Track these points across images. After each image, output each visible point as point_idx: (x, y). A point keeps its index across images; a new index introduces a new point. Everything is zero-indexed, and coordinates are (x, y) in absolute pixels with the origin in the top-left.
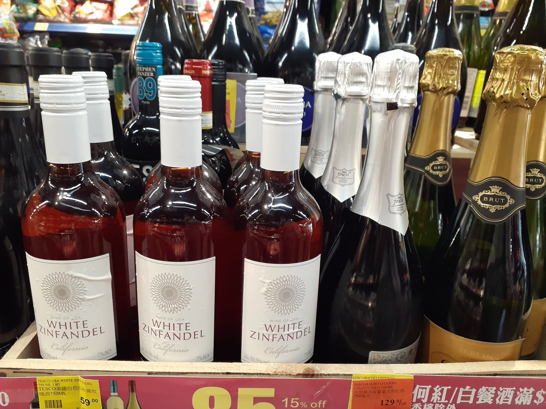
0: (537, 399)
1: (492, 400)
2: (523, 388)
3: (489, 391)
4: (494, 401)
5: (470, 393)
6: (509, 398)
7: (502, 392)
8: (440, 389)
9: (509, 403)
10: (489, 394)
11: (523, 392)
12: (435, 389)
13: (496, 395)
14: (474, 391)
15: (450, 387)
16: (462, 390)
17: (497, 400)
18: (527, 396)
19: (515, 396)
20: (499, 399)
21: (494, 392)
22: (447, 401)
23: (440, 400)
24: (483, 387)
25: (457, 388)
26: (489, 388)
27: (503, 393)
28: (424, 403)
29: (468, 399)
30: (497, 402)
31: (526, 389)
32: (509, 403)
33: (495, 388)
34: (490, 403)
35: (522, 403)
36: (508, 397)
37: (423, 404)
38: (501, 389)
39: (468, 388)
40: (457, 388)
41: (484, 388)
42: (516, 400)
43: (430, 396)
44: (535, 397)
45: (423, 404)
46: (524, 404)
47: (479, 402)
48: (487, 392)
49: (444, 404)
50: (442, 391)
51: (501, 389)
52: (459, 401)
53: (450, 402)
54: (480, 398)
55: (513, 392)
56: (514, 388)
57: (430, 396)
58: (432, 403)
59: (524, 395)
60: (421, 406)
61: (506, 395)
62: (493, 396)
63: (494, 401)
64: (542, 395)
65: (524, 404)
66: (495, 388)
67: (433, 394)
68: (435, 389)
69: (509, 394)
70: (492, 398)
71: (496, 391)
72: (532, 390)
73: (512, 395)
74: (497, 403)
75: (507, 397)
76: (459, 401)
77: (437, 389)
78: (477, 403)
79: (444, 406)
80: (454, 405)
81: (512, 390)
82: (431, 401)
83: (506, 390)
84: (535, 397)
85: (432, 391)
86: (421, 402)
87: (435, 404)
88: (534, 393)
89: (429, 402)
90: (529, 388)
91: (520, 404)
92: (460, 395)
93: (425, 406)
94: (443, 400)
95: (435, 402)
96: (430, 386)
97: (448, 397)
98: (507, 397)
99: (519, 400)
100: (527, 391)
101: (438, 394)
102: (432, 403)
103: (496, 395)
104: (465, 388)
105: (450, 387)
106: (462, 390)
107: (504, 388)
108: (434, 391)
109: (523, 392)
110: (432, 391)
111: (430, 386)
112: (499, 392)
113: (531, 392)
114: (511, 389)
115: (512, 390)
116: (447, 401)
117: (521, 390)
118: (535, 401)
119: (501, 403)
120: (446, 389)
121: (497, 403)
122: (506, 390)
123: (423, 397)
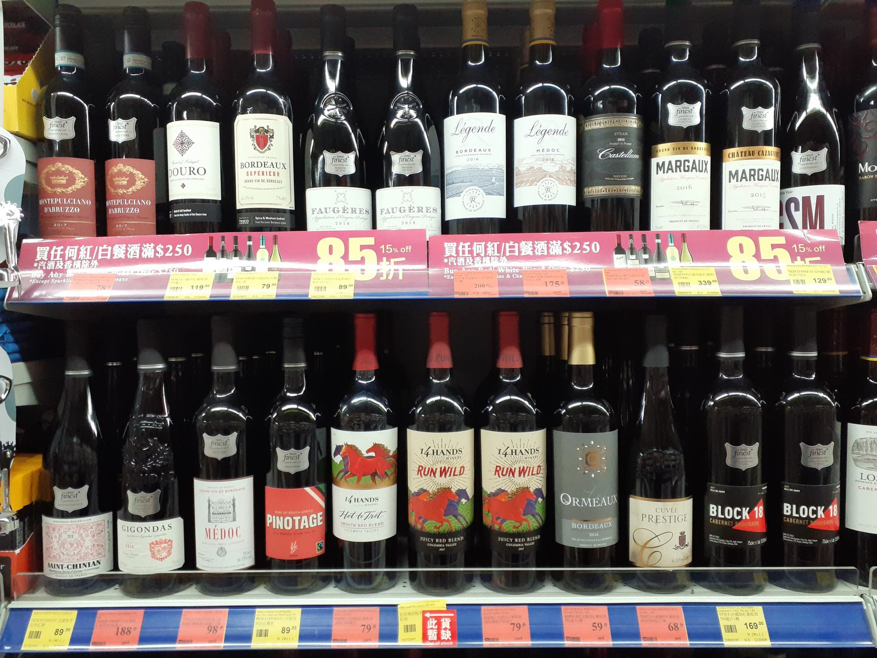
0: (158, 252)
4: (126, 256)
5: (107, 250)
8: (85, 248)
9: (138, 257)
10: (121, 250)
12: (81, 248)
13: (127, 251)
14: (110, 248)
15: (92, 247)
16: (101, 248)
17: (128, 254)
18: (150, 250)
19: (141, 251)
20: (130, 254)
21: (125, 249)
22: (91, 258)
25: (97, 247)
27: (132, 249)
29: (106, 255)
30: (129, 256)
33: (125, 245)
34: (124, 257)
37: (73, 261)
38: (129, 245)
39: (105, 247)
40: (97, 247)
41: (117, 246)
42: (143, 254)
43: (78, 255)
44: (156, 252)
46: (149, 257)
49: (89, 260)
50: (86, 250)
51: (129, 245)
52: (100, 257)
53: (94, 258)
54: (115, 253)
55: (139, 248)
56: (139, 245)
57: (78, 255)
62: (124, 252)
63: (126, 256)
65: (149, 257)
66: (125, 245)
67: (80, 253)
68: (81, 248)
71: (127, 247)
72: (152, 245)
73: (139, 250)
75: (135, 252)
77: (83, 248)
78: (114, 258)
79: (89, 262)
84: (156, 252)
85: (79, 250)
88: (155, 248)
89: (77, 259)
91: (146, 257)
92: (100, 252)
93: (75, 262)
94: (88, 257)
95: (82, 259)
96: (77, 247)
97: (91, 255)
98: (135, 252)
102: (80, 260)
103: (127, 251)
105: (92, 247)
106: (101, 248)
110: (79, 250)
111: (77, 247)
112: (128, 249)
113: (152, 247)
114: (136, 245)
116: (91, 258)
118: (157, 254)
119: (132, 257)
120: (89, 247)
123: (72, 255)
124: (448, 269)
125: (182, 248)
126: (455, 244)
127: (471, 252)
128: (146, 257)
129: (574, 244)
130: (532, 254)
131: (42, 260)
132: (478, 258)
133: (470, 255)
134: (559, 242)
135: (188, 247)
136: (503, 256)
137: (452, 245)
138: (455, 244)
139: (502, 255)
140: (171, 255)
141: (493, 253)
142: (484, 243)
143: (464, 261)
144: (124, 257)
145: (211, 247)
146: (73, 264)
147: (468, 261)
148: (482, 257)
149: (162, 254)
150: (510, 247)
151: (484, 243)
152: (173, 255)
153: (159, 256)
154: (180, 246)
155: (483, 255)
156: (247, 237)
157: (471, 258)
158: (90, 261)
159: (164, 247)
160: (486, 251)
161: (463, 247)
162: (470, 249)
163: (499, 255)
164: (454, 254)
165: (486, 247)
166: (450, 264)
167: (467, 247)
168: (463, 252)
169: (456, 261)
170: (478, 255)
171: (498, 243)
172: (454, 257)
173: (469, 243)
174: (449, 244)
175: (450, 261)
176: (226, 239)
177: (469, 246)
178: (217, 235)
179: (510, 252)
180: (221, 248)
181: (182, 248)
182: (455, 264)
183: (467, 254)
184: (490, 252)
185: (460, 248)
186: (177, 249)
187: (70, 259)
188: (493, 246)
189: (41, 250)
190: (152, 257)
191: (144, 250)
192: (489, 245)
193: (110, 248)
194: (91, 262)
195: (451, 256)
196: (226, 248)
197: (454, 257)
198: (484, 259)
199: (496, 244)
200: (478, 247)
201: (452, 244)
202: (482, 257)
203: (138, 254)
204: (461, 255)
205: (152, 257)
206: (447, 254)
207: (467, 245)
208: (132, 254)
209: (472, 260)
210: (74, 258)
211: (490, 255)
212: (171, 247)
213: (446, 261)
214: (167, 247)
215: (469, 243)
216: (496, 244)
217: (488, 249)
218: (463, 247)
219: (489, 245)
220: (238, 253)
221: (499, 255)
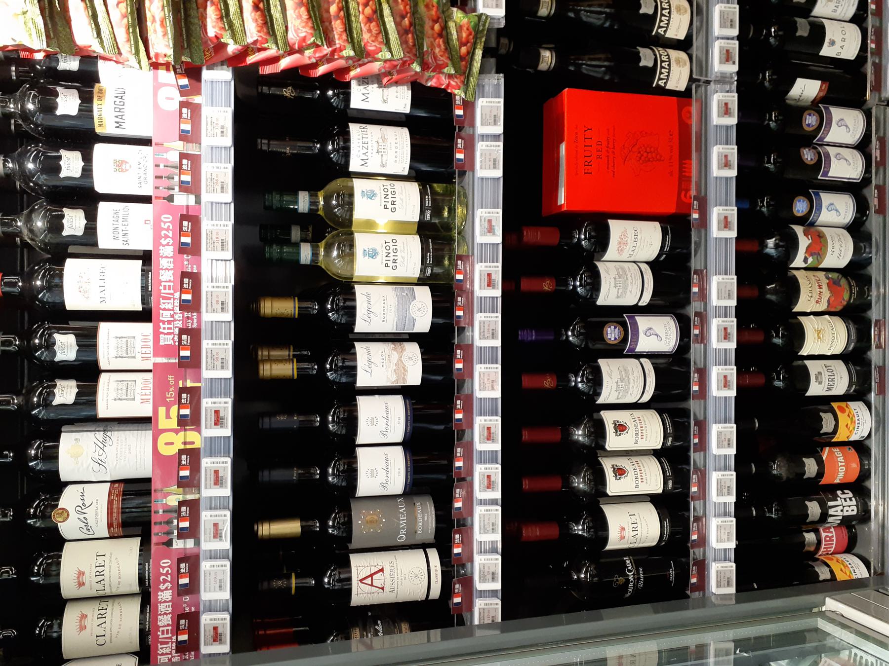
0: (167, 587)
4: (169, 614)
5: (163, 631)
9: (170, 604)
12: (160, 653)
13: (165, 614)
16: (161, 637)
18: (164, 595)
19: (165, 602)
31: (159, 597)
32: (170, 604)
33: (159, 617)
38: (160, 612)
41: (159, 624)
42: (168, 600)
45: (172, 657)
47: (170, 623)
50: (162, 648)
51: (160, 612)
55: (162, 604)
56: (159, 605)
58: (171, 652)
62: (165, 616)
63: (169, 614)
68: (160, 653)
71: (160, 615)
76: (170, 635)
84: (166, 589)
86: (171, 658)
88: (162, 591)
102: (171, 652)
103: (165, 614)
108: (163, 653)
113: (162, 593)
117: (160, 600)
125: (163, 568)
126: (161, 336)
127: (169, 322)
129: (163, 236)
130: (173, 271)
133: (172, 323)
134: (161, 248)
138: (161, 336)
145: (163, 544)
146: (175, 656)
149: (169, 584)
150: (165, 289)
152: (169, 574)
153: (170, 586)
154: (161, 570)
155: (172, 312)
157: (175, 323)
160: (169, 310)
161: (164, 328)
162: (166, 323)
163: (172, 299)
164: (171, 337)
165: (164, 309)
167: (164, 326)
168: (169, 328)
170: (172, 316)
171: (161, 299)
172: (174, 337)
173: (161, 324)
174: (161, 341)
177: (164, 324)
179: (169, 289)
180: (165, 535)
181: (163, 568)
183: (171, 326)
184: (170, 307)
185: (166, 331)
186: (165, 572)
188: (164, 303)
190: (171, 591)
191: (164, 599)
192: (162, 306)
193: (161, 629)
196: (165, 531)
197: (174, 337)
199: (162, 301)
201: (161, 338)
202: (175, 313)
203: (168, 604)
204: (172, 331)
205: (171, 591)
206: (171, 342)
208: (168, 609)
209: (177, 322)
215: (161, 324)
216: (162, 301)
218: (164, 328)
219: (162, 306)
221: (172, 299)
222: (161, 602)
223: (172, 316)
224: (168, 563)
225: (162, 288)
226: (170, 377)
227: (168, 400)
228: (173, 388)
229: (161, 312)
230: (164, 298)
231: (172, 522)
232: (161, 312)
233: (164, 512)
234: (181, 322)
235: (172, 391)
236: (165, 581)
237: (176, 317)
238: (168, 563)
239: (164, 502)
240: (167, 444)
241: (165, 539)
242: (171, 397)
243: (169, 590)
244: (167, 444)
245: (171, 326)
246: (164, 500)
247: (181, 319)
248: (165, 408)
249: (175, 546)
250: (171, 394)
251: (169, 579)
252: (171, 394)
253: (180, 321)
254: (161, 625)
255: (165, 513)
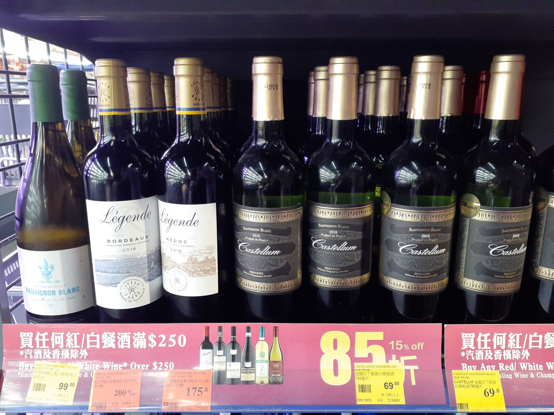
0: (150, 342)
1: (115, 344)
2: (137, 333)
3: (110, 337)
4: (117, 345)
5: (95, 338)
6: (127, 342)
7: (120, 336)
9: (129, 347)
10: (110, 338)
11: (137, 336)
12: (67, 335)
13: (117, 341)
16: (88, 336)
18: (141, 339)
19: (132, 341)
20: (120, 344)
21: (114, 337)
23: (74, 345)
24: (105, 333)
25: (84, 334)
26: (109, 333)
28: (62, 349)
30: (119, 346)
31: (139, 334)
33: (114, 333)
34: (114, 347)
35: (139, 347)
36: (127, 341)
38: (119, 334)
41: (105, 334)
42: (134, 343)
44: (148, 342)
46: (141, 348)
48: (109, 337)
49: (77, 348)
50: (73, 337)
51: (119, 334)
53: (82, 347)
54: (105, 342)
55: (129, 337)
56: (129, 333)
59: (139, 340)
60: (59, 351)
61: (124, 341)
62: (114, 341)
63: (117, 345)
64: (154, 338)
65: (141, 348)
66: (114, 333)
69: (127, 339)
70: (114, 342)
74: (119, 347)
80: (85, 350)
81: (128, 335)
82: (67, 346)
83: (123, 335)
84: (148, 342)
85: (65, 338)
87: (70, 349)
88: (146, 337)
90: (141, 333)
91: (138, 348)
92: (88, 341)
95: (70, 347)
98: (125, 342)
99: (136, 343)
100: (141, 336)
101: (70, 340)
103: (117, 341)
104: (90, 334)
106: (88, 336)
107: (121, 333)
108: (67, 338)
109: (137, 336)
112: (118, 337)
113: (143, 337)
114: (127, 334)
115: (128, 335)
117: (135, 334)
118: (149, 345)
119: (123, 347)
121: (119, 347)
122: (123, 335)
124: (466, 365)
125: (176, 339)
127: (490, 344)
128: (138, 348)
131: (27, 348)
132: (498, 351)
135: (182, 337)
136: (525, 349)
137: (470, 336)
138: (473, 335)
139: (524, 348)
140: (164, 345)
141: (514, 345)
142: (505, 334)
143: (482, 355)
144: (114, 347)
145: (207, 338)
147: (487, 354)
148: (502, 350)
151: (505, 334)
152: (167, 346)
153: (152, 346)
154: (174, 336)
156: (245, 329)
157: (490, 351)
158: (79, 349)
159: (157, 336)
161: (483, 338)
162: (490, 340)
163: (521, 347)
166: (468, 359)
167: (486, 338)
169: (475, 355)
170: (499, 347)
171: (521, 334)
173: (489, 334)
175: (468, 355)
176: (223, 330)
178: (214, 326)
179: (533, 344)
180: (218, 340)
181: (176, 339)
182: (473, 359)
183: (486, 347)
184: (511, 344)
186: (171, 340)
187: (57, 347)
188: (515, 338)
189: (25, 336)
190: (145, 347)
191: (136, 339)
192: (511, 336)
193: (98, 336)
194: (79, 352)
195: (469, 349)
196: (223, 340)
197: (472, 350)
198: (504, 352)
199: (518, 335)
200: (499, 339)
202: (502, 350)
203: (129, 344)
204: (479, 347)
205: (145, 347)
206: (465, 346)
207: (486, 336)
208: (123, 344)
209: (491, 354)
210: (62, 346)
211: (511, 348)
212: (164, 337)
213: (463, 354)
214: (159, 336)
215: (489, 334)
216: (518, 335)
217: (509, 341)
219: (511, 336)
220: (236, 344)
221: (521, 347)
222: (132, 335)
223: (499, 347)
224: (182, 343)
225: (535, 335)
226: (422, 345)
227: (393, 342)
228: (407, 347)
229: (504, 335)
230: (522, 339)
231: (233, 348)
232: (504, 335)
233: (248, 338)
234: (492, 359)
235: (403, 348)
236: (158, 340)
237: (498, 352)
238: (182, 343)
239: (261, 339)
240: (335, 341)
241: (214, 340)
242: (395, 346)
243: (147, 345)
244: (335, 341)
245: (486, 347)
246: (263, 339)
247: (496, 359)
248: (382, 339)
249: (202, 351)
250: (399, 347)
251: (161, 345)
252: (399, 347)
253: (493, 356)
254: (103, 335)
255: (246, 339)
